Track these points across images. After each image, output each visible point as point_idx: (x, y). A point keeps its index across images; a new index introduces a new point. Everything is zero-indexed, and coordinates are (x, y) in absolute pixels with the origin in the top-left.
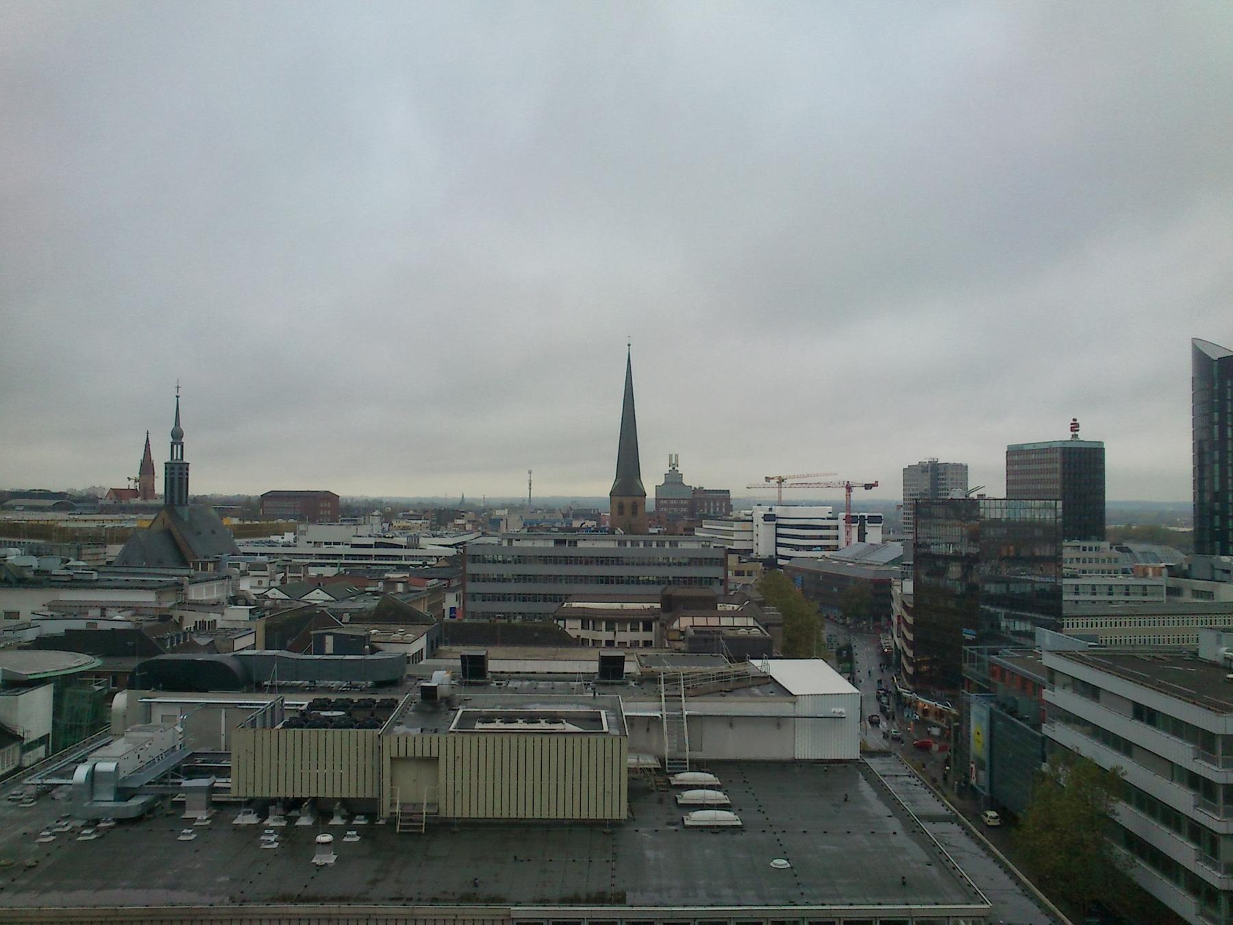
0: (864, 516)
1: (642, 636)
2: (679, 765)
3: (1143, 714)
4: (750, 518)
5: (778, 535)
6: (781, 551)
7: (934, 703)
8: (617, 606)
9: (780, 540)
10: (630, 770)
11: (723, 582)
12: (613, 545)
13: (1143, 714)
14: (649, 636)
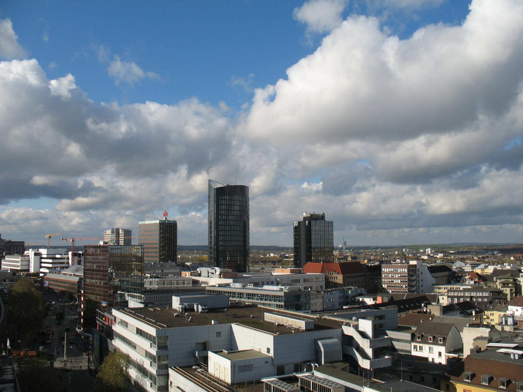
0: (80, 253)
3: (140, 332)
4: (28, 254)
5: (41, 263)
6: (42, 270)
7: (90, 335)
9: (43, 265)
13: (140, 332)
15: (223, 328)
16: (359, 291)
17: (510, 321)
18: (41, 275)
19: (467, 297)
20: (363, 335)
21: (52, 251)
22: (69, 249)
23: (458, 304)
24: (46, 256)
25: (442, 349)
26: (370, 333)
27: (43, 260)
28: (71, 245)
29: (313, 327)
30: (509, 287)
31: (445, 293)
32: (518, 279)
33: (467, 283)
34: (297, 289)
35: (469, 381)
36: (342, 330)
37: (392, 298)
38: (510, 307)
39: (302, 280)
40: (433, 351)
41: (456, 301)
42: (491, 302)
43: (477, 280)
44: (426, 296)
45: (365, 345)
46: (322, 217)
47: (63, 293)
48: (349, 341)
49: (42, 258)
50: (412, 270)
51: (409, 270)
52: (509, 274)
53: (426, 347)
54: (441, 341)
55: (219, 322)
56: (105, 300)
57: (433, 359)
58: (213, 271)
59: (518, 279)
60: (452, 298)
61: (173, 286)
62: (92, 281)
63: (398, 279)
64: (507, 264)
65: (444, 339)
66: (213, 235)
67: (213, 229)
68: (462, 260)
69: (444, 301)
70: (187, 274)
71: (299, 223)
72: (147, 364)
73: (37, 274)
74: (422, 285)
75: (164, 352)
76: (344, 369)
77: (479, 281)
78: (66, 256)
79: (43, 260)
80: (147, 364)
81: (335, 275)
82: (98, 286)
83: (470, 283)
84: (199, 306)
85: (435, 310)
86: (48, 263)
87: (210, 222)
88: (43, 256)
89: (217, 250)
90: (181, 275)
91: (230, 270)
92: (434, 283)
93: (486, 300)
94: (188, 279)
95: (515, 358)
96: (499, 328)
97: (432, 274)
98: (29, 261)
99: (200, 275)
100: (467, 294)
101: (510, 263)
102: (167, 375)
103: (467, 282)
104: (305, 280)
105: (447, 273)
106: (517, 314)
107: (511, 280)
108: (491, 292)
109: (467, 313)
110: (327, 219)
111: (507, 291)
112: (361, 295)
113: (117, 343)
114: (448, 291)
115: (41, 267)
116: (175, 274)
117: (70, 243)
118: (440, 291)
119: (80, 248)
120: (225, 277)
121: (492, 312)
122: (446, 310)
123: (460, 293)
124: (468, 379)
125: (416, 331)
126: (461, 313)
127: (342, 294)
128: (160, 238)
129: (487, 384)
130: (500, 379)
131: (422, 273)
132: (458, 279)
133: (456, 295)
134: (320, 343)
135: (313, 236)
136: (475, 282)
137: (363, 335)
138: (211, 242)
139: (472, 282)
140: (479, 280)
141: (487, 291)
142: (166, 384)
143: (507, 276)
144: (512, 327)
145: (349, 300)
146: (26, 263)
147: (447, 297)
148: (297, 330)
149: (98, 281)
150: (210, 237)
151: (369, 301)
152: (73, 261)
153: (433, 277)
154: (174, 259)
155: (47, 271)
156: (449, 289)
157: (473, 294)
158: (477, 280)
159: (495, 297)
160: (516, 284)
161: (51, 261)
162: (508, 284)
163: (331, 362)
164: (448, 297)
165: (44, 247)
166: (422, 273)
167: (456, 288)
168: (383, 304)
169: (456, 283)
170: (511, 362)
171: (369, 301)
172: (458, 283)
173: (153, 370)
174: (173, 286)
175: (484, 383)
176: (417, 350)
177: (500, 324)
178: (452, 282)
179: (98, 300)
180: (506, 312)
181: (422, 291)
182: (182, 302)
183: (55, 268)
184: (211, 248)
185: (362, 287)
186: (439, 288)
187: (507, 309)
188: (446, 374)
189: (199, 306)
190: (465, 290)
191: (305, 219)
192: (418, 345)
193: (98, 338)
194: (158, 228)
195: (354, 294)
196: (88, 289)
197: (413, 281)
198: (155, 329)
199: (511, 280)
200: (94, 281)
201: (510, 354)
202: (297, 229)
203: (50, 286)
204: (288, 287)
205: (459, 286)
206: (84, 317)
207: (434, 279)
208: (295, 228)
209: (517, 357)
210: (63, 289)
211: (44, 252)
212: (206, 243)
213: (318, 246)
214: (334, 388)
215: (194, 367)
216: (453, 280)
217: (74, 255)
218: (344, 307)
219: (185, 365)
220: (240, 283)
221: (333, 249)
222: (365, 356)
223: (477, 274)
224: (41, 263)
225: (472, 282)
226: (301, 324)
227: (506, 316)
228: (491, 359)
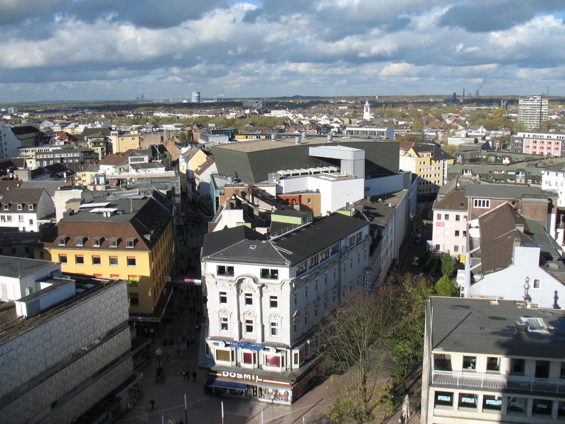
17: (102, 180)
19: (57, 159)
25: (34, 216)
30: (100, 146)
31: (33, 156)
32: (109, 137)
33: (56, 144)
35: (64, 245)
38: (101, 167)
40: (23, 219)
41: (45, 164)
42: (82, 163)
43: (67, 140)
44: (12, 161)
52: (100, 133)
53: (15, 216)
54: (31, 208)
57: (24, 228)
59: (109, 137)
64: (98, 122)
68: (51, 119)
69: (33, 165)
74: (6, 149)
77: (69, 142)
83: (60, 144)
85: (22, 175)
92: (20, 146)
93: (77, 161)
95: (107, 216)
96: (91, 188)
97: (17, 136)
100: (57, 156)
101: (101, 121)
103: (56, 143)
105: (34, 134)
106: (108, 173)
107: (102, 139)
108: (82, 152)
109: (58, 176)
111: (98, 150)
114: (37, 154)
118: (27, 154)
121: (83, 173)
122: (35, 174)
123: (49, 155)
124: (63, 243)
126: (51, 176)
129: (82, 245)
130: (94, 238)
131: (5, 135)
132: (47, 140)
133: (45, 157)
136: (65, 143)
139: (62, 143)
140: (69, 140)
141: (78, 152)
143: (97, 135)
144: (104, 186)
147: (35, 160)
153: (19, 140)
156: (37, 151)
158: (67, 140)
159: (86, 157)
160: (107, 143)
162: (99, 143)
164: (37, 160)
166: (5, 135)
167: (45, 150)
169: (45, 145)
170: (104, 221)
172: (47, 145)
175: (78, 245)
176: (5, 221)
177: (93, 184)
178: (40, 143)
180: (98, 172)
181: (7, 155)
186: (26, 151)
187: (99, 169)
188: (39, 241)
190: (55, 152)
192: (6, 215)
199: (102, 139)
201: (102, 213)
205: (48, 148)
207: (20, 141)
209: (109, 215)
216: (41, 141)
223: (67, 134)
225: (62, 143)
227: (98, 176)
228: (85, 220)
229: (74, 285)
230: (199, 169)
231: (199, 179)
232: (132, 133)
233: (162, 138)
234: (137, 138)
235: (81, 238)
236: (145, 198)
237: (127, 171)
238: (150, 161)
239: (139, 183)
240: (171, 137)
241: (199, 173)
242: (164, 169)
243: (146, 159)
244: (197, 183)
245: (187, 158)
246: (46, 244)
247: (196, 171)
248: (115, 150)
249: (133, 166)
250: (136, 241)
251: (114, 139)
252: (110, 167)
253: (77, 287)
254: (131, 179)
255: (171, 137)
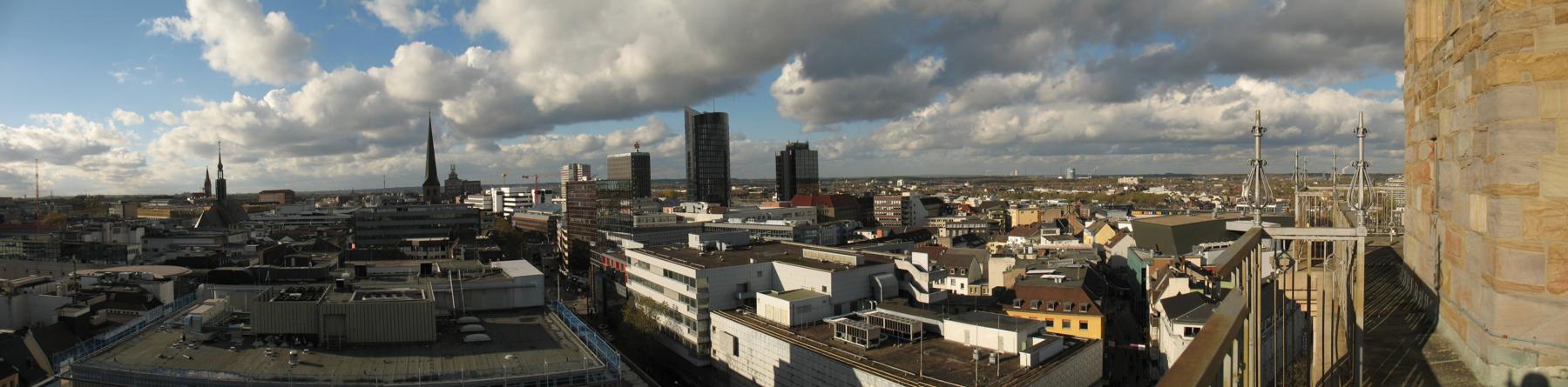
1: (440, 253)
2: (459, 313)
3: (668, 274)
5: (504, 202)
6: (506, 209)
8: (428, 239)
9: (506, 204)
10: (437, 318)
11: (479, 225)
12: (424, 209)
13: (668, 274)
14: (444, 253)
15: (764, 266)
16: (856, 224)
18: (506, 214)
20: (919, 268)
21: (514, 190)
22: (531, 186)
23: (964, 236)
24: (508, 195)
25: (965, 281)
26: (925, 266)
27: (506, 199)
28: (533, 182)
29: (863, 263)
33: (959, 215)
34: (805, 223)
36: (895, 265)
37: (892, 231)
38: (1010, 238)
39: (793, 214)
42: (991, 234)
43: (969, 212)
45: (922, 279)
46: (806, 146)
47: (532, 234)
48: (903, 275)
49: (504, 197)
50: (906, 203)
51: (902, 203)
55: (759, 260)
56: (593, 240)
57: (955, 291)
58: (700, 206)
60: (951, 230)
61: (670, 222)
62: (577, 219)
63: (891, 211)
65: (967, 270)
66: (692, 167)
67: (692, 161)
70: (669, 211)
71: (782, 152)
72: (683, 308)
73: (501, 214)
75: (705, 296)
76: (905, 304)
78: (529, 194)
79: (506, 199)
80: (683, 308)
81: (826, 208)
82: (584, 225)
84: (723, 244)
86: (511, 202)
87: (689, 153)
88: (506, 195)
89: (697, 183)
90: (661, 211)
91: (719, 205)
93: (983, 231)
94: (673, 216)
98: (492, 200)
99: (684, 211)
100: (965, 226)
102: (709, 320)
104: (796, 214)
105: (938, 205)
110: (811, 148)
112: (858, 228)
113: (633, 286)
114: (947, 223)
115: (504, 206)
116: (652, 211)
117: (532, 181)
119: (543, 185)
120: (713, 213)
124: (1018, 305)
125: (937, 264)
127: (838, 228)
128: (633, 171)
134: (877, 279)
135: (797, 168)
136: (968, 214)
137: (919, 268)
138: (689, 175)
139: (965, 214)
142: (706, 329)
145: (846, 235)
146: (489, 202)
148: (852, 268)
149: (584, 220)
150: (689, 170)
151: (868, 235)
152: (536, 199)
154: (648, 193)
155: (512, 210)
157: (972, 226)
158: (969, 212)
161: (514, 200)
162: (999, 215)
163: (890, 298)
165: (506, 186)
168: (880, 240)
171: (868, 235)
173: (693, 316)
174: (670, 222)
179: (585, 240)
182: (701, 240)
183: (519, 207)
184: (690, 181)
185: (860, 220)
188: (998, 303)
189: (723, 244)
190: (963, 222)
191: (788, 148)
193: (601, 279)
194: (630, 161)
195: (851, 228)
196: (574, 228)
197: (907, 213)
198: (694, 271)
200: (580, 220)
202: (779, 160)
203: (518, 226)
204: (795, 222)
205: (952, 218)
206: (569, 258)
208: (777, 158)
209: (1060, 281)
210: (533, 229)
211: (506, 190)
212: (683, 175)
213: (803, 177)
214: (913, 324)
215: (738, 311)
217: (537, 193)
218: (849, 242)
219: (728, 308)
220: (739, 218)
221: (817, 180)
222: (921, 290)
223: (968, 205)
224: (504, 202)
225: (965, 214)
226: (853, 260)
229: (1062, 342)
230: (1109, 242)
231: (1110, 252)
232: (1031, 206)
233: (1062, 213)
234: (1036, 212)
235: (1036, 302)
236: (1083, 267)
237: (1039, 242)
238: (1062, 233)
239: (1069, 253)
240: (1071, 211)
241: (1111, 246)
242: (1077, 241)
243: (1058, 231)
244: (1108, 256)
245: (1094, 232)
246: (1004, 306)
247: (1106, 244)
248: (1014, 223)
249: (1047, 238)
250: (1089, 306)
251: (1013, 213)
252: (1019, 238)
253: (1064, 344)
254: (1060, 250)
255: (1071, 211)
